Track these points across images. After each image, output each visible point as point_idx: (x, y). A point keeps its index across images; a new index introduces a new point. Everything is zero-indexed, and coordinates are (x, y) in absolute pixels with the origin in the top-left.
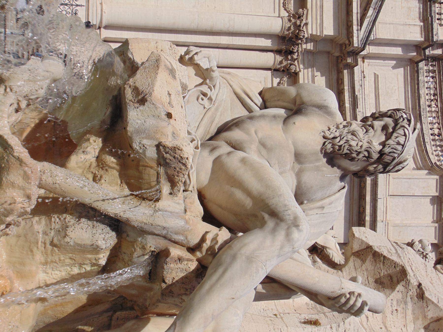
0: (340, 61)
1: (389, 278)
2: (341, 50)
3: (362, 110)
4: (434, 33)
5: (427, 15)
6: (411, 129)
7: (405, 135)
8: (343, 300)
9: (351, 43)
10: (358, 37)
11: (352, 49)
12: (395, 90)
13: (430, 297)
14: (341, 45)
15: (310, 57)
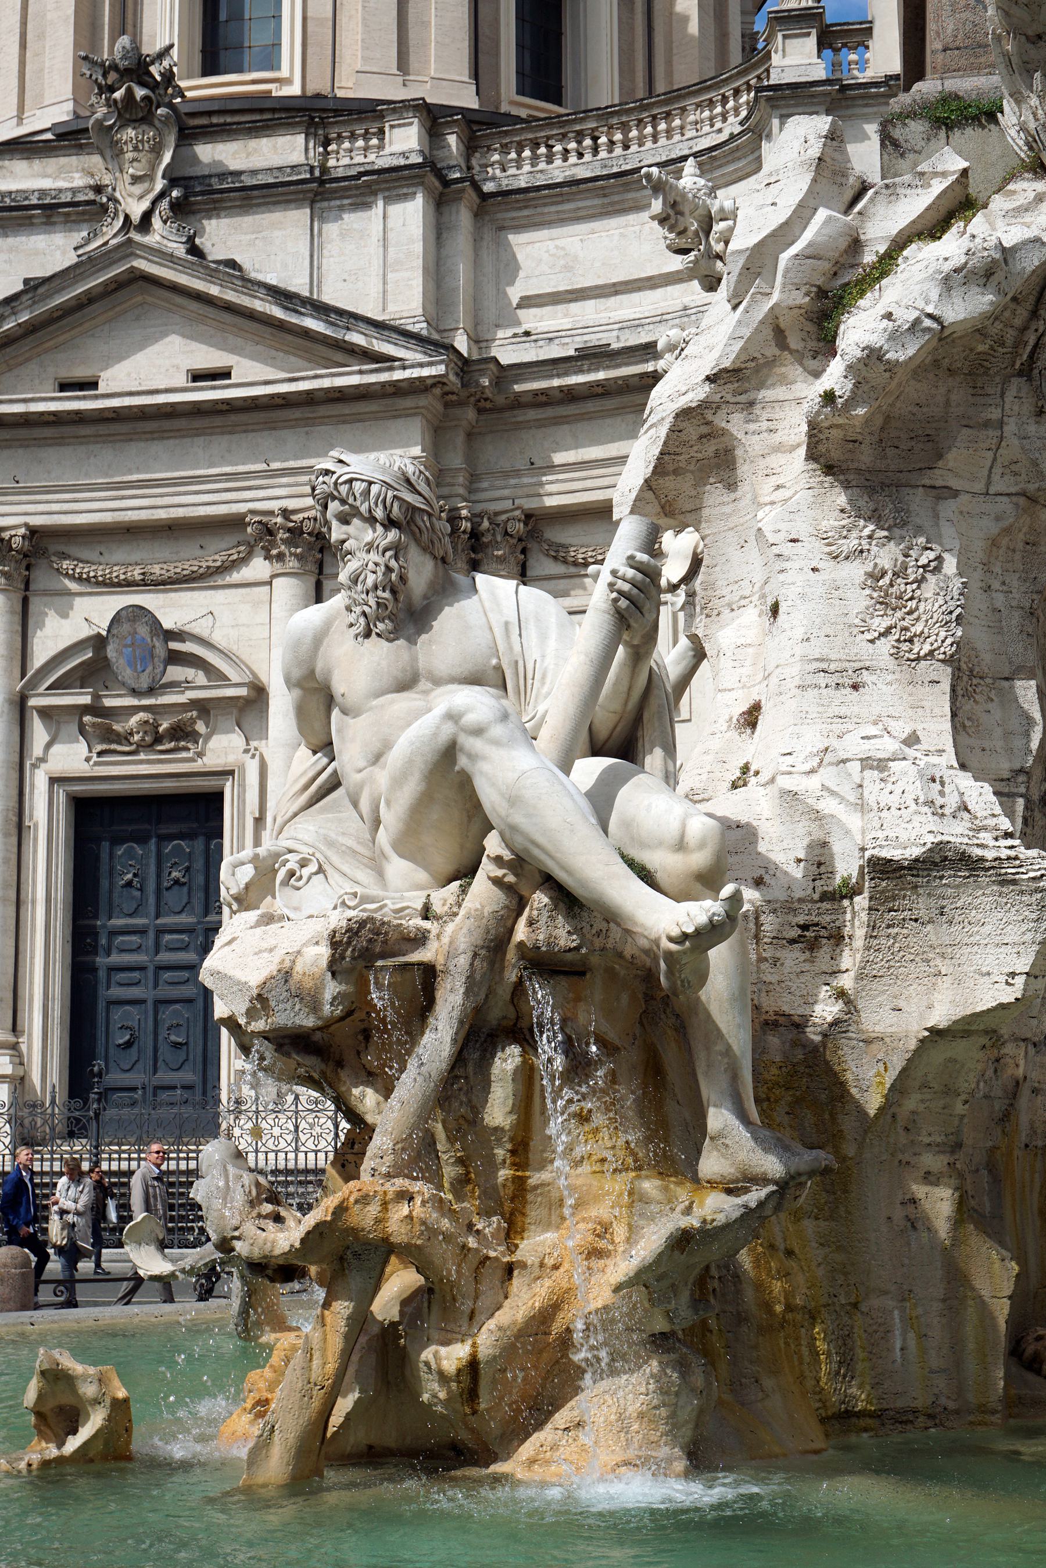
0: (488, 405)
1: (704, 440)
2: (461, 404)
3: (615, 333)
4: (402, 162)
5: (357, 187)
6: (340, 470)
7: (350, 481)
8: (623, 603)
9: (438, 382)
10: (421, 365)
11: (452, 377)
12: (557, 247)
13: (733, 356)
14: (447, 405)
15: (485, 485)
